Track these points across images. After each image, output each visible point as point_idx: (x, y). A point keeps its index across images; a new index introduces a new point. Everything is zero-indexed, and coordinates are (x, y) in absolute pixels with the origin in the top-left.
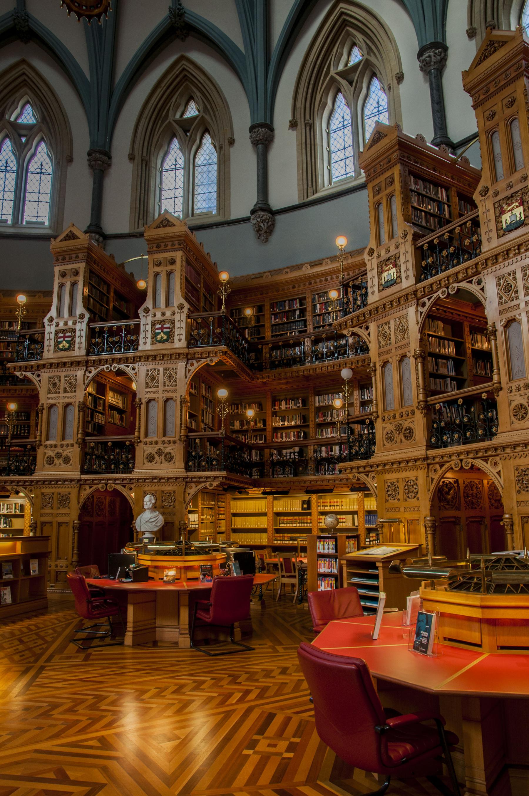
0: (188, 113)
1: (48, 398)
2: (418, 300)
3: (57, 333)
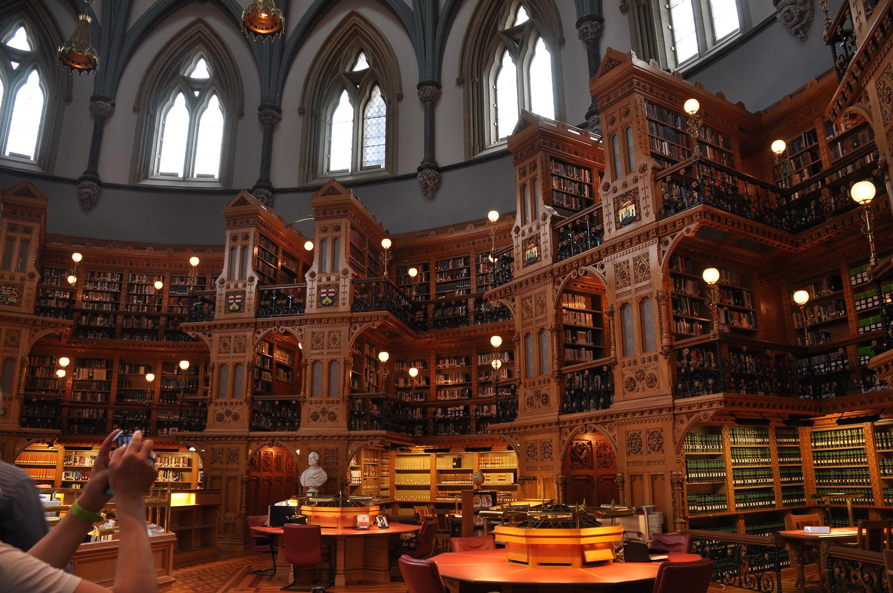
0: (358, 65)
1: (219, 358)
2: (554, 278)
3: (228, 294)
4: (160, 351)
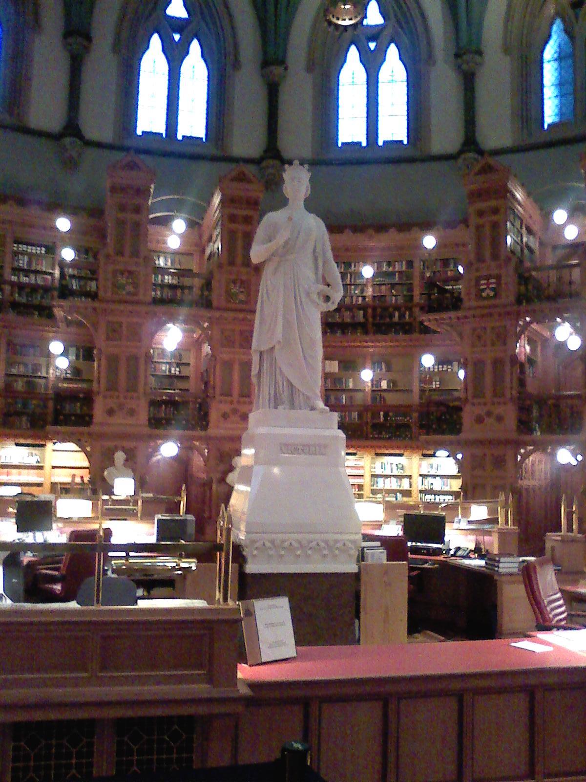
4: (368, 347)
